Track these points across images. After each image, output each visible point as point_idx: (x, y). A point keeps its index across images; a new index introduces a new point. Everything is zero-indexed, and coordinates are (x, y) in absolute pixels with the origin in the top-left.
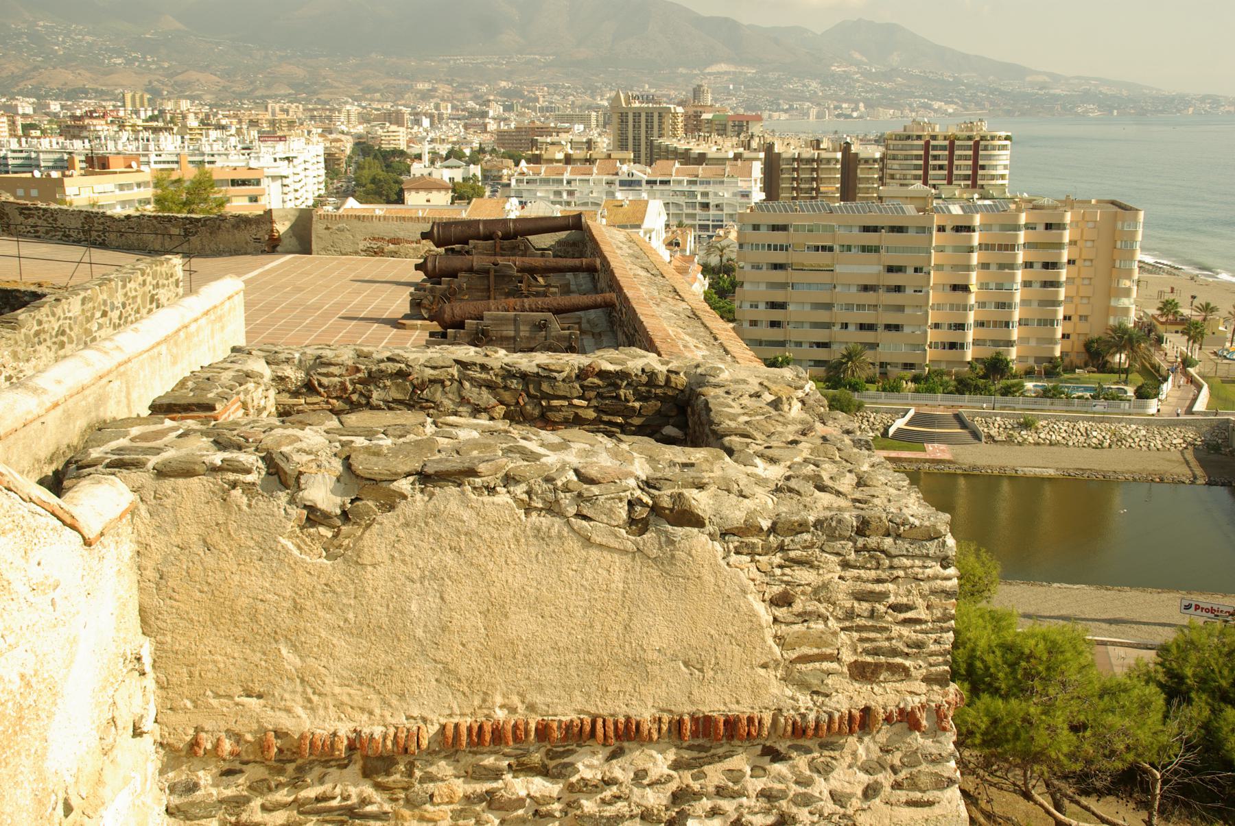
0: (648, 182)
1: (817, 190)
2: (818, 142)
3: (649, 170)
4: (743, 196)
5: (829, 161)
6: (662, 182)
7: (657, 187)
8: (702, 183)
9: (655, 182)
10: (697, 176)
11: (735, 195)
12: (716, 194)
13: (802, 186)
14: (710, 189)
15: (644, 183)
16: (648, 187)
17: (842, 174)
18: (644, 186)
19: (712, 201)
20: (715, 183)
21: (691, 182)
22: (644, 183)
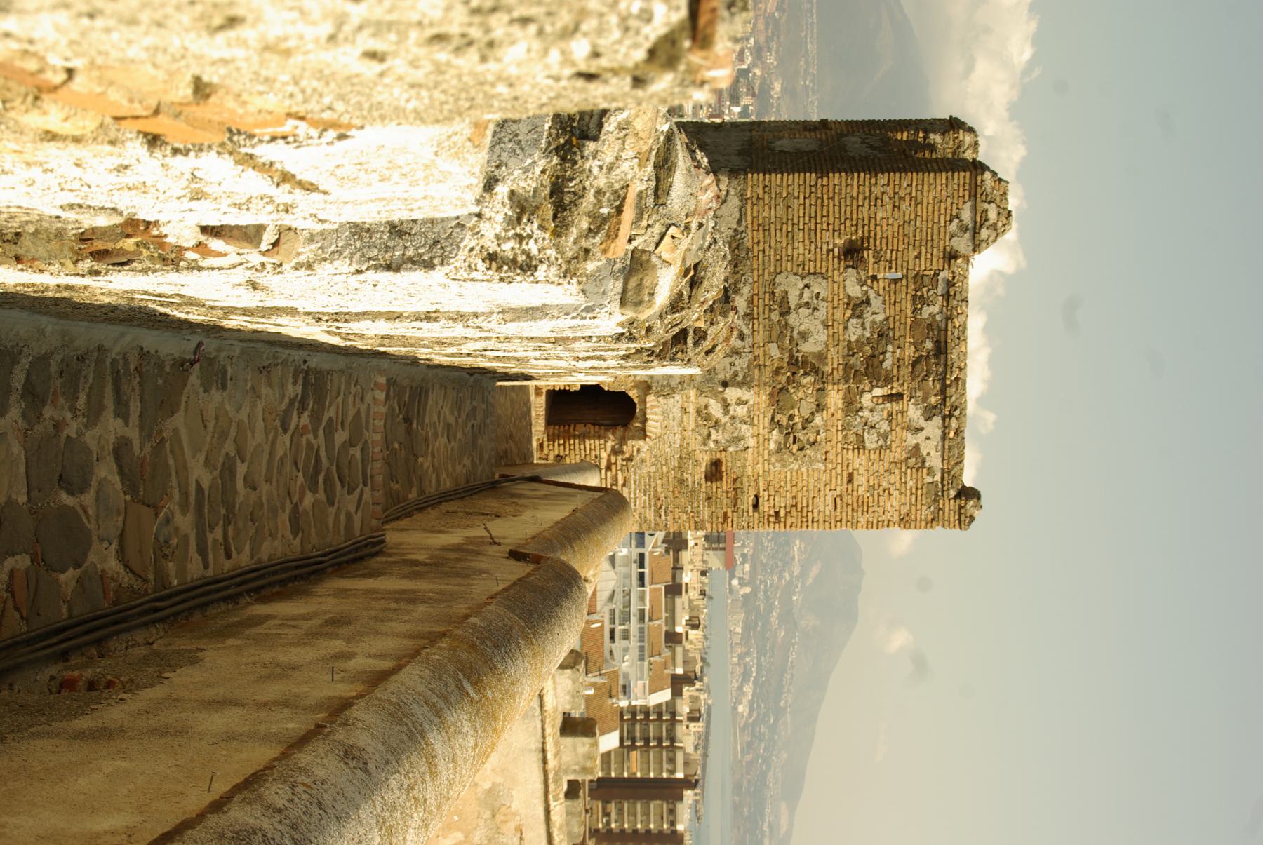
0: (642, 556)
1: (633, 747)
2: (696, 720)
3: (660, 550)
4: (624, 687)
5: (672, 760)
6: (641, 576)
7: (635, 569)
8: (641, 630)
9: (642, 565)
10: (651, 620)
11: (626, 676)
12: (626, 650)
13: (638, 727)
14: (633, 643)
15: (641, 550)
16: (635, 557)
17: (655, 780)
18: (635, 552)
19: (619, 644)
20: (642, 649)
21: (642, 612)
22: (641, 550)
